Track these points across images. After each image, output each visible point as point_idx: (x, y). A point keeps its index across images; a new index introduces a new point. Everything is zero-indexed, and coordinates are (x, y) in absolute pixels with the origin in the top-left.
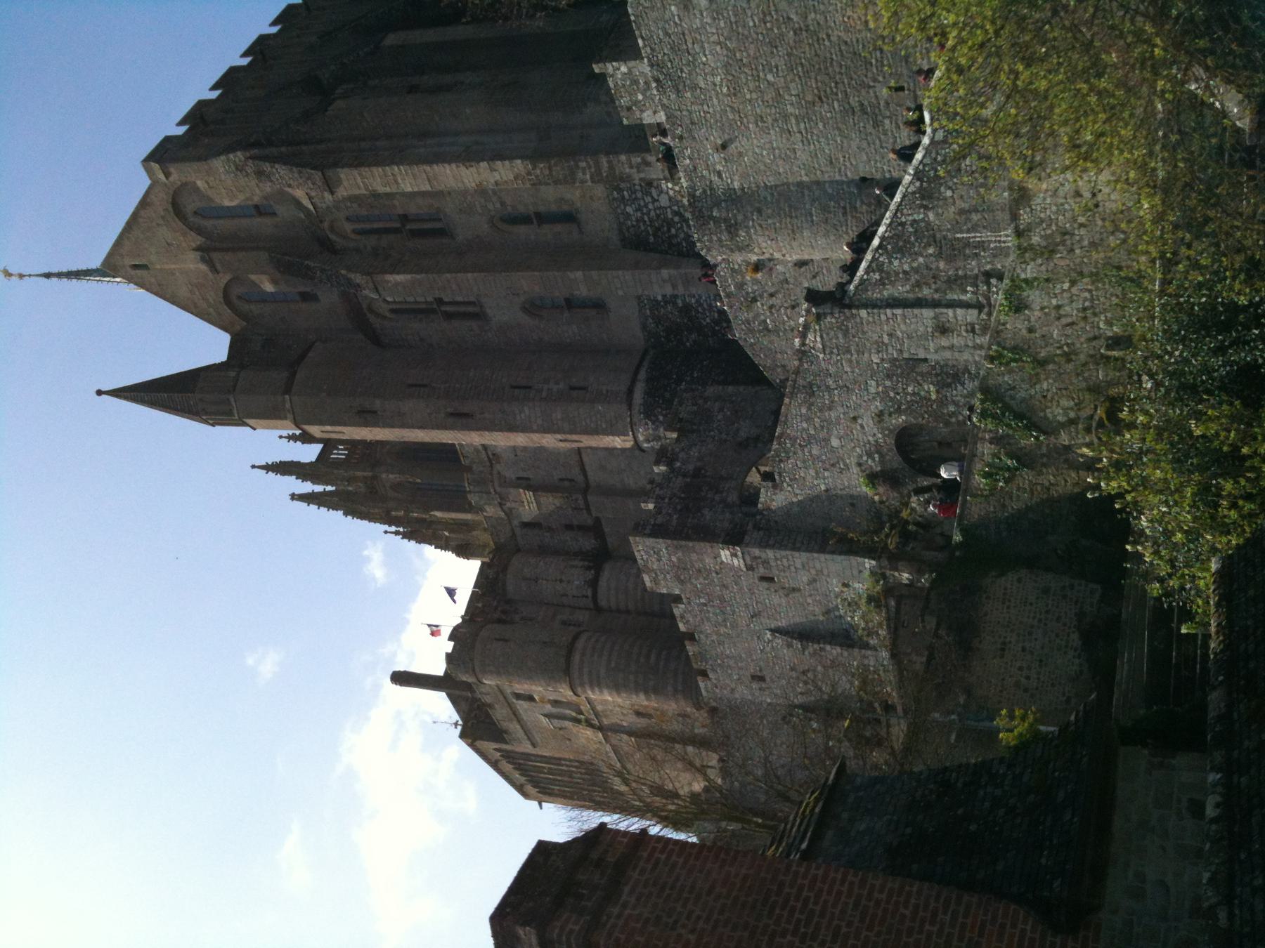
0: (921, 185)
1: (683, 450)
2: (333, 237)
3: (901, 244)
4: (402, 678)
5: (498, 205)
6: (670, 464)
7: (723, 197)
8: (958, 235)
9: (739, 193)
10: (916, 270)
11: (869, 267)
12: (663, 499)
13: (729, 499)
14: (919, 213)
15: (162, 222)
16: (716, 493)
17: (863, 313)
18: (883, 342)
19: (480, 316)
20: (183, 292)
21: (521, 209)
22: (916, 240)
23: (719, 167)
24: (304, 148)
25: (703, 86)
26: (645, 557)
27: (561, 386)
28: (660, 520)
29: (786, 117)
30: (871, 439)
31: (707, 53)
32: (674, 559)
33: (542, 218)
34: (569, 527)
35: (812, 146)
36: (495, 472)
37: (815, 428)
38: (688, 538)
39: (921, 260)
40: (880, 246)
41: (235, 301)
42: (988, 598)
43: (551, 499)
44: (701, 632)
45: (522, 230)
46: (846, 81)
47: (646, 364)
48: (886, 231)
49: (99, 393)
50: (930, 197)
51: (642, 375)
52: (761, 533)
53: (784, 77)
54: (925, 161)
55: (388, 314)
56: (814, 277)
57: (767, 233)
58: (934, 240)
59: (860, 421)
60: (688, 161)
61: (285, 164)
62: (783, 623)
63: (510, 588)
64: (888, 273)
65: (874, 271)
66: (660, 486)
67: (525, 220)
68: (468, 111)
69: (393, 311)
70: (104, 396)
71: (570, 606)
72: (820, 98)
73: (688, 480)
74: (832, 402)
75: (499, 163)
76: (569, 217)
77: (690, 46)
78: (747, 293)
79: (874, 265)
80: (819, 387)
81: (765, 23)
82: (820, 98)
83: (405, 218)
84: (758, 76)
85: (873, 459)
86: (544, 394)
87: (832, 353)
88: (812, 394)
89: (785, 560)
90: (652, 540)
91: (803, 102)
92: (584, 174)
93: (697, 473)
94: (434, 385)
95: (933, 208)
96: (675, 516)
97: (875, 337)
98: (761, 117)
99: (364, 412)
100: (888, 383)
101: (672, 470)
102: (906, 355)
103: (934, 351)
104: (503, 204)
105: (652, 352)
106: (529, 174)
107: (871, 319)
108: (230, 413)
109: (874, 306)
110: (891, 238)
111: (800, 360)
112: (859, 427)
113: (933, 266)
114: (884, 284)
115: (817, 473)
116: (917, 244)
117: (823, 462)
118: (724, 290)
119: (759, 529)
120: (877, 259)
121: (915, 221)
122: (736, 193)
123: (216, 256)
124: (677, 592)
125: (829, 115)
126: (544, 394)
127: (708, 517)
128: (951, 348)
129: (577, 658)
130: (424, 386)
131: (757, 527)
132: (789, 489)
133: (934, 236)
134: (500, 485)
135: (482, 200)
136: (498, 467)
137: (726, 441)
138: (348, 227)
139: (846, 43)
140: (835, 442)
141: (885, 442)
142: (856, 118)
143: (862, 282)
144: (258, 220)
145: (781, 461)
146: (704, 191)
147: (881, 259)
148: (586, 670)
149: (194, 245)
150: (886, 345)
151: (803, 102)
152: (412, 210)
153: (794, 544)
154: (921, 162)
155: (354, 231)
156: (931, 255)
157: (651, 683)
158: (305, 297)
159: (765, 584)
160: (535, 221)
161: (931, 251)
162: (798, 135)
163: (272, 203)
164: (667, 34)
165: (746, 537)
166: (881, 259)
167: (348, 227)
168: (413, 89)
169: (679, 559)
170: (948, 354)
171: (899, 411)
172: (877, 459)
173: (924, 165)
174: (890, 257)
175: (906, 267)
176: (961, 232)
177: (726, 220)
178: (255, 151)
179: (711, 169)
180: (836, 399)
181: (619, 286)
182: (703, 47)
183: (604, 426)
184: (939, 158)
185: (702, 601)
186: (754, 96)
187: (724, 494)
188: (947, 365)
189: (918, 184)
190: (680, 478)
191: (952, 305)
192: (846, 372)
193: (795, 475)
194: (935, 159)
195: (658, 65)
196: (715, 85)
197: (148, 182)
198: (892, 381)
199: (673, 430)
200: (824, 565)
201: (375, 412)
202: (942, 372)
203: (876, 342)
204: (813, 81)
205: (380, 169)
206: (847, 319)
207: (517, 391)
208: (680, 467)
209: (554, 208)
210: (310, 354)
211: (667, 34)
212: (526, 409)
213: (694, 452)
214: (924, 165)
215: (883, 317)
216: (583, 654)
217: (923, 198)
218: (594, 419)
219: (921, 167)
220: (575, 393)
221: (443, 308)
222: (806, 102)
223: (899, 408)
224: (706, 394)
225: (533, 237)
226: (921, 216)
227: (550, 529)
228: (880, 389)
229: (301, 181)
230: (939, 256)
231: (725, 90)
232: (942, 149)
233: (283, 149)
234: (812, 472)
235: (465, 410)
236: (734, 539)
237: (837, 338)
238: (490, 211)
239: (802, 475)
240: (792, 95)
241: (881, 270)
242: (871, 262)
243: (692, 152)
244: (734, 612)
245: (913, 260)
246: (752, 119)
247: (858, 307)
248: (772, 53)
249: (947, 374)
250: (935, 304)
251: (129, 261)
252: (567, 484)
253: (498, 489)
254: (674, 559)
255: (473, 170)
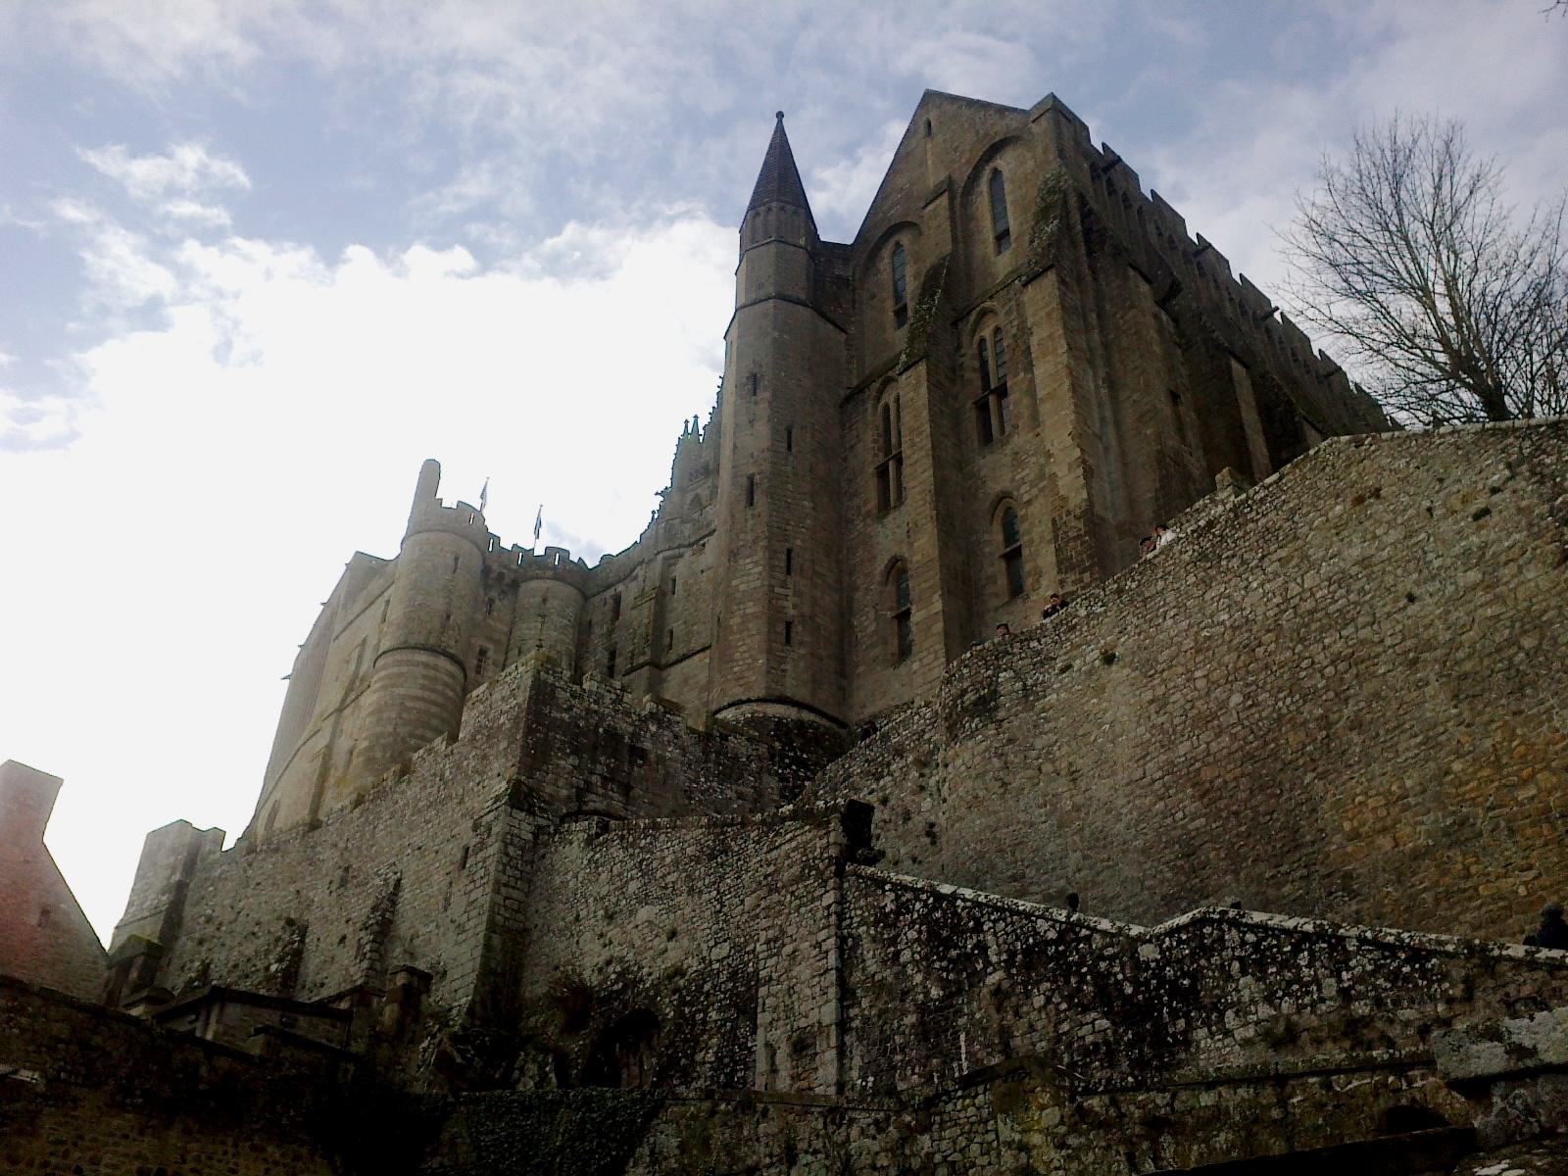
0: (1052, 942)
1: (676, 737)
2: (973, 317)
3: (945, 933)
4: (431, 473)
5: (1026, 498)
6: (652, 716)
7: (1030, 682)
8: (963, 1037)
9: (1039, 705)
10: (902, 974)
11: (905, 888)
12: (595, 702)
13: (593, 797)
14: (999, 954)
15: (982, 132)
16: (605, 779)
17: (830, 898)
18: (784, 945)
19: (885, 507)
20: (901, 181)
21: (1023, 528)
22: (950, 961)
23: (1077, 663)
24: (1083, 250)
25: (1207, 597)
26: (508, 679)
27: (792, 612)
28: (562, 695)
29: (1169, 745)
30: (645, 971)
31: (1267, 586)
32: (502, 720)
33: (1013, 557)
34: (613, 655)
35: (1121, 802)
36: (682, 550)
37: (663, 877)
38: (529, 731)
39: (919, 978)
40: (939, 897)
41: (893, 241)
42: (297, 1158)
43: (646, 621)
44: (409, 782)
45: (1000, 537)
46: (1243, 829)
47: (824, 722)
48: (964, 900)
49: (780, 115)
50: (1028, 966)
51: (807, 716)
52: (530, 837)
53: (1240, 721)
54: (1097, 936)
55: (882, 402)
56: (914, 860)
57: (978, 759)
58: (952, 991)
59: (671, 945)
60: (1083, 612)
61: (1059, 229)
62: (406, 895)
63: (534, 584)
64: (894, 926)
65: (898, 898)
66: (619, 700)
67: (1011, 535)
68: (1148, 432)
69: (887, 408)
70: (776, 120)
71: (506, 659)
72: (1206, 793)
73: (627, 740)
74: (701, 892)
75: (1080, 471)
76: (1016, 590)
77: (1275, 557)
78: (889, 764)
79: (909, 895)
80: (722, 865)
81: (1333, 662)
82: (1206, 793)
83: (1002, 392)
84: (1236, 680)
85: (616, 982)
86: (777, 590)
87: (768, 865)
88: (712, 857)
89: (482, 872)
90: (529, 682)
91: (1198, 765)
92: (1074, 583)
93: (643, 754)
94: (791, 458)
95: (1010, 976)
96: (566, 716)
97: (791, 930)
98: (1165, 705)
99: (755, 379)
100: (723, 977)
101: (644, 720)
102: (763, 991)
103: (770, 1034)
104: (1029, 502)
105: (843, 732)
106: (1068, 513)
107: (819, 915)
108: (753, 240)
109: (841, 916)
110: (955, 913)
111: (763, 822)
112: (662, 946)
113: (909, 1005)
114: (876, 924)
115: (602, 898)
116: (945, 964)
117: (617, 904)
118: (893, 728)
119: (536, 836)
120: (917, 899)
121: (982, 947)
122: (1038, 700)
123: (944, 200)
124: (461, 735)
125: (1180, 815)
126: (777, 590)
127: (563, 762)
128: (774, 1070)
129: (422, 657)
130: (789, 448)
131: (539, 830)
132: (585, 862)
133: (960, 992)
134: (665, 559)
135: (1032, 476)
136: (688, 552)
137: (690, 798)
138: (987, 332)
139: (1314, 810)
140: (644, 913)
141: (639, 994)
142: (1179, 863)
143: (880, 883)
144: (988, 234)
145: (622, 838)
146: (1039, 653)
147: (918, 906)
148: (404, 669)
149: (955, 176)
150: (778, 954)
151: (1198, 765)
152: (1014, 396)
153: (505, 885)
154: (1094, 930)
155: (982, 340)
156: (927, 993)
157: (379, 755)
158: (901, 313)
159: (459, 856)
160: (1008, 549)
161: (935, 992)
162: (1138, 774)
163: (1013, 245)
164: (1293, 512)
165: (524, 814)
166: (918, 906)
167: (987, 332)
168: (1174, 397)
169: (504, 723)
170: (762, 1065)
171: (683, 1003)
172: (615, 987)
173: (1088, 939)
174: (925, 919)
175: (906, 956)
176: (970, 1042)
177: (995, 694)
178: (1073, 200)
179: (1075, 653)
180: (705, 897)
181: (925, 661)
182: (1276, 575)
183: (736, 669)
184: (1103, 965)
185: (447, 773)
186: (1201, 684)
187: (601, 791)
188: (746, 1069)
189: (1052, 935)
190: (631, 729)
191: (842, 1052)
192: (742, 901)
193: (602, 865)
194: (1102, 958)
195: (1236, 516)
196: (1211, 617)
197: (1027, 108)
198: (729, 979)
199: (707, 727)
200: (471, 932)
201: (755, 394)
202: (736, 1063)
203: (783, 932)
204: (1238, 771)
205: (1061, 331)
206: (821, 873)
207: (784, 557)
208: (648, 729)
209: (1028, 567)
210: (830, 327)
211: (1293, 512)
212: (760, 569)
213: (672, 752)
214: (1088, 939)
215: (822, 935)
216: (426, 666)
217: (1028, 952)
218: (747, 655)
219: (1084, 932)
220: (781, 628)
221: (892, 465)
222: (1199, 769)
223: (686, 1004)
224: (766, 778)
225: (987, 550)
226: (994, 959)
227: (610, 633)
228: (716, 966)
229: (1039, 250)
230: (922, 1009)
231: (1205, 633)
232: (1123, 966)
233: (1079, 227)
234: (604, 892)
235: (759, 498)
236: (520, 797)
237: (790, 867)
238: (1018, 490)
239: (603, 876)
240: (1208, 744)
241: (902, 908)
242: (913, 890)
243: (1100, 614)
244: (427, 822)
245: (916, 963)
246: (1161, 690)
247: (839, 888)
248: (1280, 690)
249: (734, 1071)
250: (843, 1025)
251: (933, 116)
252: (667, 641)
253: (660, 556)
254: (502, 720)
255: (1069, 441)
